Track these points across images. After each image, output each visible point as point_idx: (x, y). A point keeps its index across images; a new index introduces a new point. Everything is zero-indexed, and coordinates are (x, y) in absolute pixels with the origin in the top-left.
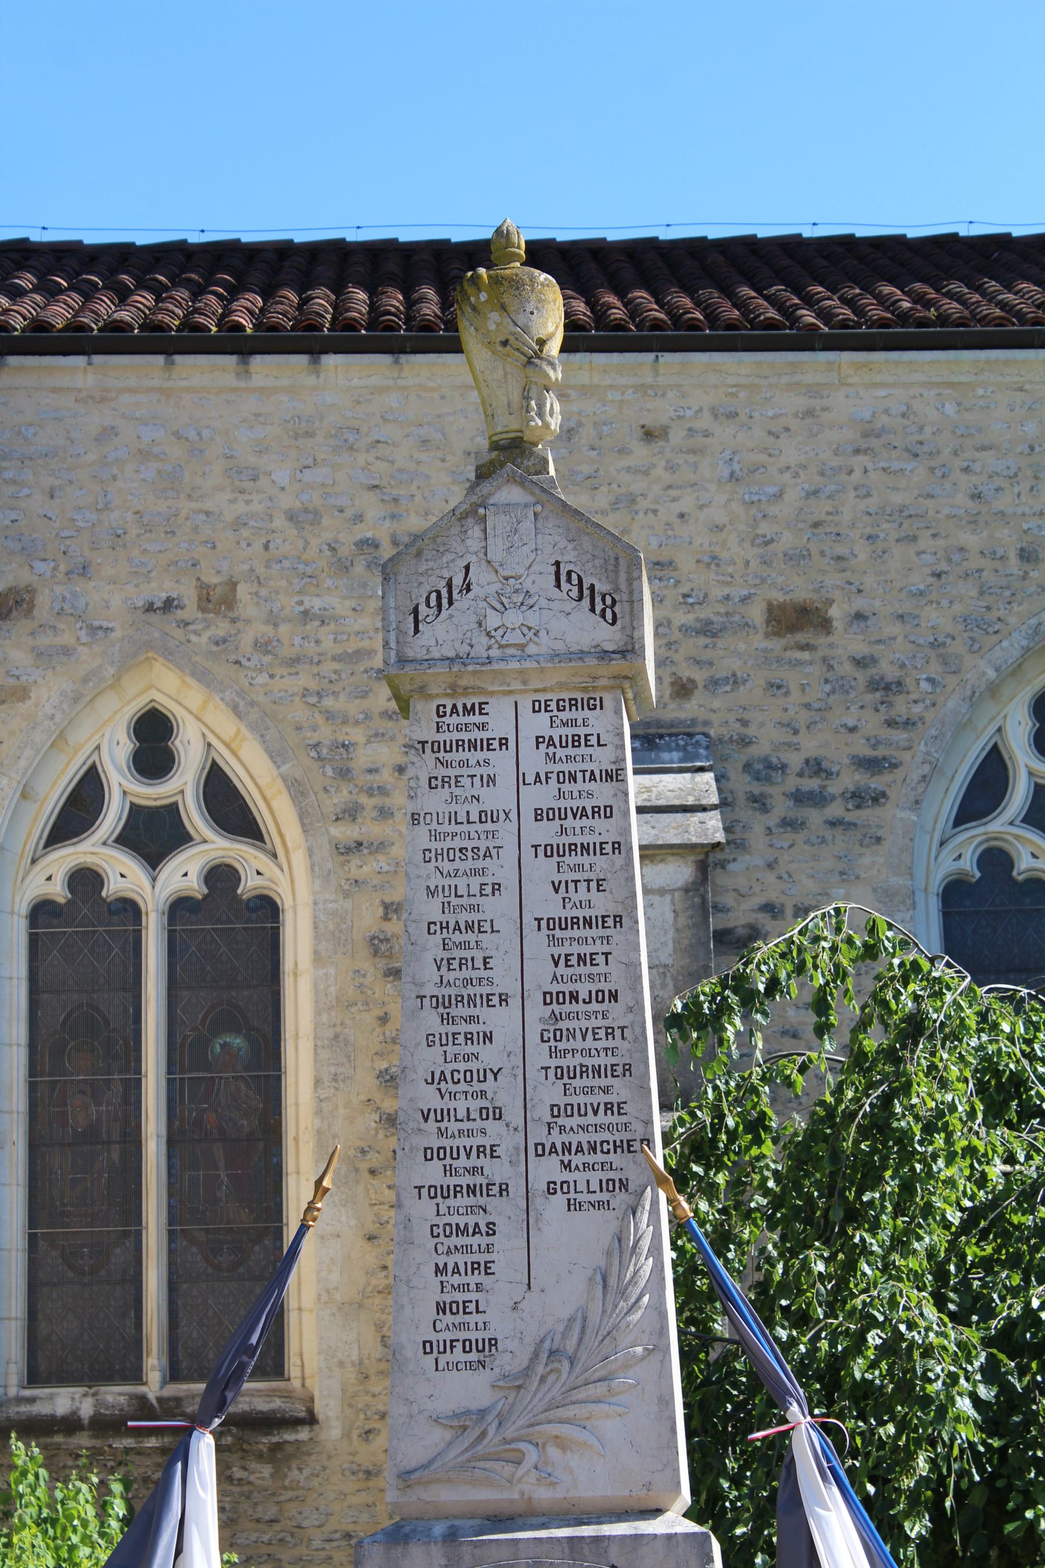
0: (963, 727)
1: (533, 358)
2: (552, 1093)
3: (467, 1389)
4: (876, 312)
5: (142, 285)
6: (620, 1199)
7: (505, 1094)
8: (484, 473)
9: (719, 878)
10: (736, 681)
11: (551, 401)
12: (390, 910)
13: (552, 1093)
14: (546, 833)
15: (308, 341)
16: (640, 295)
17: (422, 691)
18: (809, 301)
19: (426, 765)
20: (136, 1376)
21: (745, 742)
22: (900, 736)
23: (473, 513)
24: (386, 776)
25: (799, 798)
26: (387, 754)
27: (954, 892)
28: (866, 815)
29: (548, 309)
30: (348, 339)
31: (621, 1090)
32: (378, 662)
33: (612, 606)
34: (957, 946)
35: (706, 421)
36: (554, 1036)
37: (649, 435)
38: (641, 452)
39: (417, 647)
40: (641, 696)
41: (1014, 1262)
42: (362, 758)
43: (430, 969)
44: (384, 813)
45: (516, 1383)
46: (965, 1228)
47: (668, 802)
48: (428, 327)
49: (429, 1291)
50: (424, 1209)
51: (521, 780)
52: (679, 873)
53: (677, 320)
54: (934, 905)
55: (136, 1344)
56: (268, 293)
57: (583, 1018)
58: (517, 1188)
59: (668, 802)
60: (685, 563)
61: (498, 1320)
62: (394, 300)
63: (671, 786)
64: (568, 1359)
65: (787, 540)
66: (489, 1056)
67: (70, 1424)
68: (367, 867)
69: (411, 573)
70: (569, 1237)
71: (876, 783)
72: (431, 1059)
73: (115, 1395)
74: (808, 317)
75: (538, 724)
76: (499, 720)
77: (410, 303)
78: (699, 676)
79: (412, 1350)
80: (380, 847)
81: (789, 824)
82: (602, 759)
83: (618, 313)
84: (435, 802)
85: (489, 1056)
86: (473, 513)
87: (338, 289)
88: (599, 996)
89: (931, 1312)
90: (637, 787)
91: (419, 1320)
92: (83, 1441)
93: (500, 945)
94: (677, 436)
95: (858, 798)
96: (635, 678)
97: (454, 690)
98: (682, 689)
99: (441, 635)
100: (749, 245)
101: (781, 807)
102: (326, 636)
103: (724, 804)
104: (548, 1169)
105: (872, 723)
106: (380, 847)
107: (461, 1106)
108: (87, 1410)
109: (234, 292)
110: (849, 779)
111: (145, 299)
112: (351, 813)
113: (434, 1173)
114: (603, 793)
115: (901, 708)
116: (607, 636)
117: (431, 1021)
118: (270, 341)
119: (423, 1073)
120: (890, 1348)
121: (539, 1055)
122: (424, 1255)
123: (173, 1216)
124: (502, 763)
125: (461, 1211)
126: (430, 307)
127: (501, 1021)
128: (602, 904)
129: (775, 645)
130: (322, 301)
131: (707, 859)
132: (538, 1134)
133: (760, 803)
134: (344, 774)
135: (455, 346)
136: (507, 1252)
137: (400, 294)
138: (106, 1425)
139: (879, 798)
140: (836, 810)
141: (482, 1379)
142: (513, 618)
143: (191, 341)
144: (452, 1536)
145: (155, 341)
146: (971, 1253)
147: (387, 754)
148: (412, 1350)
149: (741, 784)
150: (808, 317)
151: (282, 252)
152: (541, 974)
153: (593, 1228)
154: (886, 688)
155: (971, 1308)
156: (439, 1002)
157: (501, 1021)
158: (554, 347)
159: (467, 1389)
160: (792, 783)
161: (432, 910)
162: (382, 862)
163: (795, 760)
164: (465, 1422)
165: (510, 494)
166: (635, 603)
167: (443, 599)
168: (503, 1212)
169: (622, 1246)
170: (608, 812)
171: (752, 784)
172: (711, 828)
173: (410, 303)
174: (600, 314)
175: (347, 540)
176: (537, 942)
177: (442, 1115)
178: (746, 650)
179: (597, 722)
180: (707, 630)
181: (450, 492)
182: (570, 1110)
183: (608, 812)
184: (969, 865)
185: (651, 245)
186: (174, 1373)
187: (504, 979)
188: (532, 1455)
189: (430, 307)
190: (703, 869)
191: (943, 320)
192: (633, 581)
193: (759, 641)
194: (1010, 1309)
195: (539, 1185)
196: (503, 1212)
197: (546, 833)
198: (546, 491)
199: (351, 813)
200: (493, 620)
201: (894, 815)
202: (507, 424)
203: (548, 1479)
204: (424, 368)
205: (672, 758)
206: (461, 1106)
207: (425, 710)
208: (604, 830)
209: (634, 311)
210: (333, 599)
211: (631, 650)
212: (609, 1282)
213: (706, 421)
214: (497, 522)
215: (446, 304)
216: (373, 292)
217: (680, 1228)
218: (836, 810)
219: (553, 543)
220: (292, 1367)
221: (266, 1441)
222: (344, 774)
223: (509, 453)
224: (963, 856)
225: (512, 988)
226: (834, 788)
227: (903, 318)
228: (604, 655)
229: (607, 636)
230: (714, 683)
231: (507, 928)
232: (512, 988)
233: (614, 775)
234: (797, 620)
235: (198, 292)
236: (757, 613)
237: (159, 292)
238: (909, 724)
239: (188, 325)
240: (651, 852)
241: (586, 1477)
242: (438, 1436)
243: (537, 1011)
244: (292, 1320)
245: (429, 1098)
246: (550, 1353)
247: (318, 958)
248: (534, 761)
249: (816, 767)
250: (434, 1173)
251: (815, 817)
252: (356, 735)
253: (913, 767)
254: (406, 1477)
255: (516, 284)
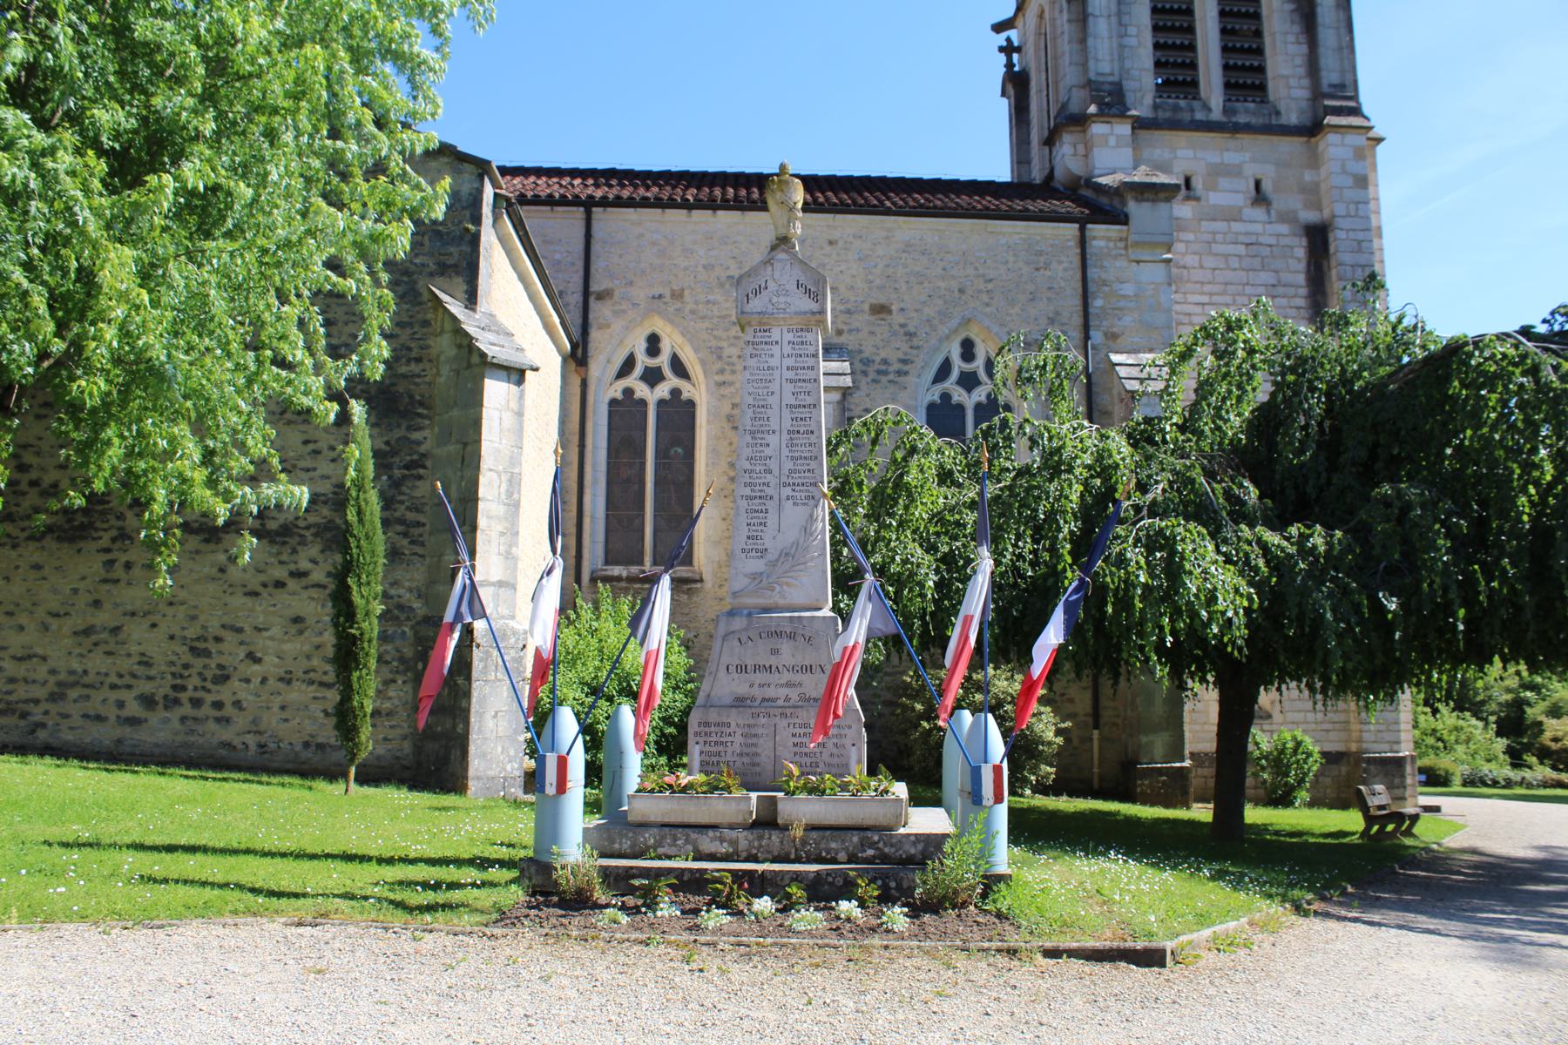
0: (937, 349)
1: (792, 209)
2: (790, 465)
3: (755, 565)
4: (912, 203)
5: (655, 184)
6: (812, 502)
7: (773, 465)
8: (773, 248)
9: (849, 399)
10: (858, 330)
11: (798, 224)
12: (734, 406)
13: (790, 465)
14: (791, 375)
15: (712, 205)
16: (830, 194)
17: (749, 323)
18: (889, 199)
19: (750, 349)
20: (641, 563)
21: (860, 352)
22: (915, 352)
23: (768, 262)
24: (734, 359)
25: (879, 372)
26: (734, 351)
27: (931, 408)
28: (902, 379)
29: (799, 195)
30: (726, 205)
31: (813, 465)
32: (734, 319)
33: (816, 296)
34: (931, 423)
35: (850, 239)
36: (791, 445)
37: (831, 243)
38: (828, 249)
39: (748, 308)
40: (825, 329)
41: (946, 533)
42: (726, 352)
43: (745, 423)
44: (733, 372)
45: (774, 564)
46: (930, 521)
47: (833, 372)
48: (754, 202)
49: (745, 531)
50: (743, 504)
51: (782, 356)
52: (836, 396)
53: (842, 203)
54: (924, 411)
55: (642, 553)
56: (699, 189)
57: (801, 439)
58: (776, 498)
59: (833, 372)
60: (842, 289)
61: (768, 542)
62: (743, 192)
63: (834, 366)
64: (792, 556)
65: (878, 282)
66: (768, 451)
67: (619, 579)
68: (726, 391)
69: (745, 284)
70: (793, 514)
71: (906, 368)
72: (748, 452)
73: (634, 569)
74: (888, 204)
75: (789, 337)
76: (775, 335)
77: (749, 193)
78: (845, 328)
79: (738, 551)
80: (731, 384)
81: (875, 381)
82: (811, 350)
83: (821, 199)
84: (752, 362)
85: (768, 451)
86: (768, 262)
87: (723, 188)
88: (807, 432)
89: (919, 551)
90: (823, 366)
91: (741, 541)
92: (623, 584)
93: (773, 414)
94: (841, 243)
95: (899, 373)
96: (823, 322)
97: (760, 323)
98: (839, 333)
99: (756, 304)
100: (868, 178)
101: (872, 375)
102: (715, 309)
103: (852, 373)
104: (787, 491)
105: (905, 347)
106: (731, 384)
107: (758, 468)
108: (624, 574)
109: (687, 188)
110: (896, 366)
111: (655, 189)
112: (722, 372)
113: (747, 491)
114: (811, 362)
115: (915, 342)
116: (814, 306)
117: (748, 438)
118: (699, 205)
119: (744, 456)
120: (905, 562)
121: (785, 452)
122: (743, 519)
123: (656, 509)
124: (776, 350)
125: (754, 500)
126: (756, 195)
127: (773, 440)
128: (809, 400)
129: (872, 318)
130: (718, 192)
131: (846, 392)
132: (784, 479)
133: (865, 373)
134: (720, 358)
135: (765, 208)
136: (772, 519)
137: (744, 191)
138: (631, 579)
139: (906, 373)
140: (891, 377)
141: (761, 562)
142: (782, 299)
143: (671, 204)
144: (749, 615)
145: (658, 204)
146: (932, 530)
147: (734, 351)
148: (738, 551)
149: (859, 366)
150: (888, 204)
151: (704, 175)
152: (787, 424)
153: (802, 512)
154: (910, 335)
155: (931, 548)
156: (752, 432)
157: (773, 440)
158: (800, 205)
159: (755, 565)
160: (876, 367)
161: (750, 400)
162: (732, 389)
163: (878, 359)
164: (755, 576)
165: (782, 256)
166: (825, 296)
167: (758, 291)
168: (771, 505)
169: (812, 518)
170: (812, 368)
171: (862, 366)
172: (847, 381)
173: (749, 193)
174: (815, 200)
175: (723, 275)
176: (787, 414)
177: (751, 471)
178: (863, 319)
179: (809, 337)
180: (848, 312)
181: (758, 256)
182: (795, 471)
183: (812, 368)
184: (936, 398)
185: (834, 177)
186: (655, 563)
187: (774, 425)
188: (778, 589)
189: (756, 195)
190: (844, 395)
191: (935, 207)
192: (824, 288)
193: (867, 317)
194: (946, 549)
195: (784, 496)
196: (771, 505)
197: (791, 375)
198: (795, 255)
199: (722, 372)
200: (775, 300)
201: (911, 379)
202: (782, 231)
203: (783, 597)
204: (754, 217)
205: (835, 356)
206: (758, 468)
207: (750, 330)
208: (810, 374)
209: (827, 199)
210: (718, 296)
211: (822, 312)
212: (807, 530)
213: (850, 239)
214: (777, 265)
215: (761, 193)
216: (736, 190)
217: (832, 513)
218: (891, 377)
219: (798, 273)
220: (695, 562)
221: (685, 587)
222: (720, 358)
223: (783, 241)
224: (934, 395)
225: (777, 428)
226: (891, 369)
227: (921, 206)
228: (813, 313)
229: (814, 306)
230: (850, 331)
231: (776, 408)
232: (777, 428)
233: (815, 356)
234: (880, 310)
235: (674, 187)
236: (866, 307)
237: (660, 186)
238: (918, 348)
239: (670, 199)
240: (827, 389)
241: (796, 596)
242: (747, 581)
243: (785, 436)
244: (696, 540)
245: (747, 466)
246: (785, 554)
247: (708, 422)
248: (787, 349)
249: (885, 362)
250: (747, 491)
251: (884, 379)
252: (724, 344)
253: (919, 363)
254: (735, 594)
255: (787, 182)
